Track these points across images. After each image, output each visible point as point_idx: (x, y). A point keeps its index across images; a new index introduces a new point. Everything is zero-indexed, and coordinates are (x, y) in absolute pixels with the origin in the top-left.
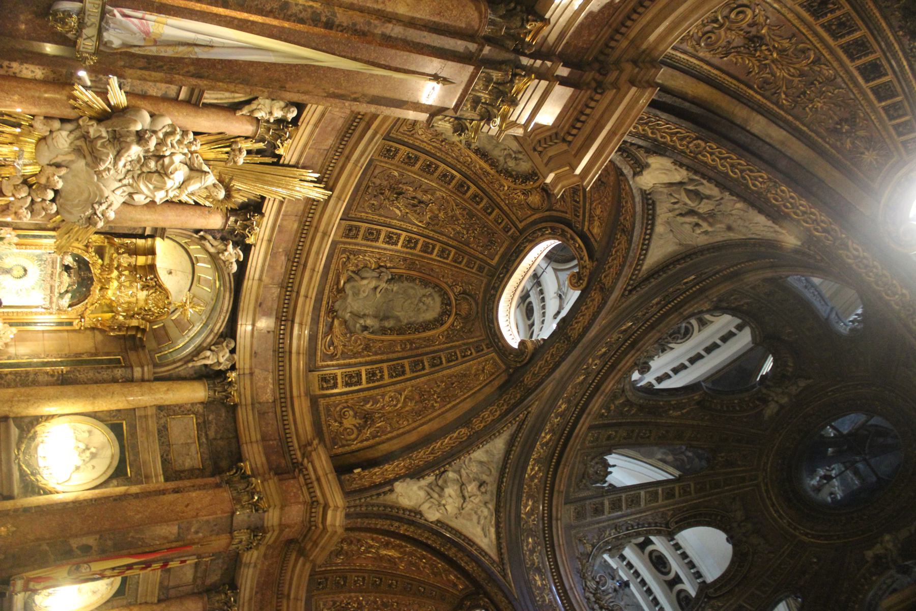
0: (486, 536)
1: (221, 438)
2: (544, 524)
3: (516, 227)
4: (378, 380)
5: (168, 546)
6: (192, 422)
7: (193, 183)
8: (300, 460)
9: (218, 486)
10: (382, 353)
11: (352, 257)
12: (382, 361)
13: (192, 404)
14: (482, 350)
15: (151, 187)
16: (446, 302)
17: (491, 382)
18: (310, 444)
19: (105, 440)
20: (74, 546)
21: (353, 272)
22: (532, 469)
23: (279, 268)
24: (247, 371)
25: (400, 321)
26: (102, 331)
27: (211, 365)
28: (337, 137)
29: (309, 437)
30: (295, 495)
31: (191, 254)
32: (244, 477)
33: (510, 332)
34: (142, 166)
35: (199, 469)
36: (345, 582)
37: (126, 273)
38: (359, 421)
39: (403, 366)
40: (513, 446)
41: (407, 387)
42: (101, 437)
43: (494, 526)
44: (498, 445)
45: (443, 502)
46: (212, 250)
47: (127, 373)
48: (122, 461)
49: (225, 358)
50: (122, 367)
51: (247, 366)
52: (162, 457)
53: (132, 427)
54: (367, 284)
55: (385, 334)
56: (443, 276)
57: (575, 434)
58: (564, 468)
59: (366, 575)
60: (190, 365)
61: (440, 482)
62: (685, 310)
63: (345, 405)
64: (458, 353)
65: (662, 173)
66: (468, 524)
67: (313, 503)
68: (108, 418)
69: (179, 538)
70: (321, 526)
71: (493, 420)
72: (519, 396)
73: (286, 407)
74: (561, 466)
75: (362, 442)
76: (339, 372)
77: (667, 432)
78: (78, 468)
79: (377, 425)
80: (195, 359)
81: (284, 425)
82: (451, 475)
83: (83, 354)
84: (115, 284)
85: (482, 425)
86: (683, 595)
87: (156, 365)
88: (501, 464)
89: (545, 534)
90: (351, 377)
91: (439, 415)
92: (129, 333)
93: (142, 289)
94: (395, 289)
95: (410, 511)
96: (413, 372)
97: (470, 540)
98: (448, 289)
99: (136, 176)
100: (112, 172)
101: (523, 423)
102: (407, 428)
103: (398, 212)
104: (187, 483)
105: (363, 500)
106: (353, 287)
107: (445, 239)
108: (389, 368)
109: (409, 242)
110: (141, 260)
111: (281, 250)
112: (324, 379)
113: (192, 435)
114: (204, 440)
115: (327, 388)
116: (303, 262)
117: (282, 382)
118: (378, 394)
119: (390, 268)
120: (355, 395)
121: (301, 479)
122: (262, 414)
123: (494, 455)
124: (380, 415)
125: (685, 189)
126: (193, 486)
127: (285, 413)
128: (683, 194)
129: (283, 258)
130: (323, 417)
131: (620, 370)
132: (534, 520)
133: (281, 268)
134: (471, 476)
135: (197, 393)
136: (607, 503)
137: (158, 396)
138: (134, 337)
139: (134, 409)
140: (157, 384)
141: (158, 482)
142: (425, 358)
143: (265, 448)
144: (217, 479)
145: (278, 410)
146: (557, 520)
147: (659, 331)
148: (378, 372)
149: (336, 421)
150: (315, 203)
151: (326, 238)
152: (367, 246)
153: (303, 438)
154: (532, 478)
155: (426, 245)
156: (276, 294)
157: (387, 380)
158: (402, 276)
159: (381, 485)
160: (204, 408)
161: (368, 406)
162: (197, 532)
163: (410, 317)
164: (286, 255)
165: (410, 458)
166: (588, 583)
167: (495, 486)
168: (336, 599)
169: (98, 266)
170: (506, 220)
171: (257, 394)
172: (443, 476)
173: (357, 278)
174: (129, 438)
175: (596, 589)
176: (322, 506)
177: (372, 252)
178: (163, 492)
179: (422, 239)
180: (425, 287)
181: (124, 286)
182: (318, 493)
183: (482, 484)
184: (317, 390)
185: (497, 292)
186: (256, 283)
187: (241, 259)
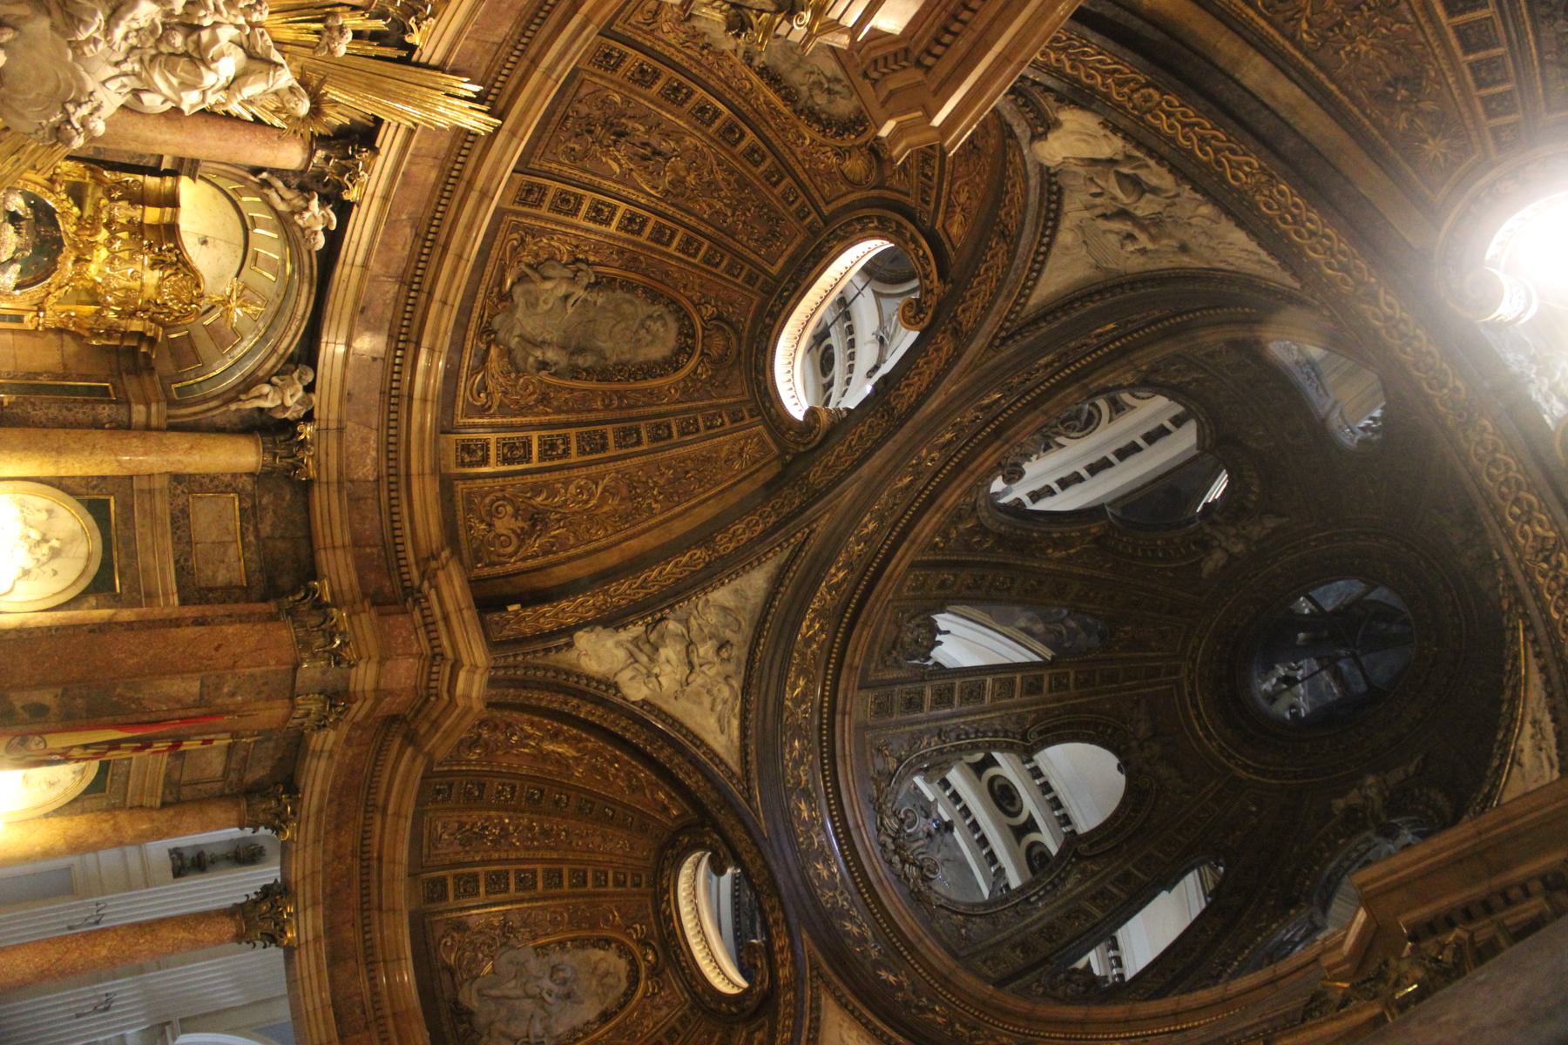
0: (722, 732)
1: (283, 538)
2: (821, 718)
3: (820, 213)
4: (560, 457)
5: (182, 713)
6: (231, 506)
7: (252, 84)
8: (417, 583)
9: (273, 618)
10: (571, 411)
11: (529, 239)
12: (568, 425)
13: (234, 475)
14: (743, 418)
15: (175, 81)
16: (686, 332)
17: (751, 474)
18: (435, 556)
19: (77, 527)
20: (18, 704)
21: (529, 266)
22: (810, 626)
23: (400, 247)
24: (333, 425)
25: (606, 359)
26: (76, 336)
27: (270, 409)
28: (517, 23)
29: (434, 546)
30: (404, 642)
31: (244, 212)
32: (319, 605)
33: (792, 393)
34: (159, 41)
35: (241, 588)
36: (481, 792)
37: (124, 235)
38: (521, 524)
39: (603, 436)
40: (781, 585)
41: (608, 472)
42: (70, 521)
44: (756, 581)
45: (656, 670)
46: (282, 207)
47: (122, 414)
48: (106, 566)
49: (295, 399)
50: (112, 402)
51: (333, 416)
52: (176, 562)
53: (127, 508)
54: (552, 289)
55: (577, 378)
56: (685, 286)
58: (862, 630)
59: (518, 783)
60: (233, 407)
61: (653, 637)
63: (499, 494)
64: (700, 420)
65: (1078, 140)
66: (695, 709)
67: (434, 657)
68: (84, 490)
69: (201, 701)
70: (446, 696)
71: (750, 540)
72: (797, 501)
73: (397, 490)
74: (858, 626)
75: (524, 559)
76: (492, 438)
77: (1040, 583)
78: (26, 573)
79: (553, 533)
80: (243, 397)
81: (393, 521)
82: (672, 626)
83: (40, 374)
84: (103, 253)
85: (732, 546)
86: (1036, 850)
87: (172, 403)
88: (758, 610)
89: (821, 735)
90: (512, 447)
91: (662, 523)
92: (126, 344)
93: (152, 267)
94: (600, 301)
95: (599, 682)
96: (621, 447)
97: (696, 737)
98: (691, 309)
99: (146, 58)
101: (801, 550)
102: (604, 542)
103: (615, 167)
104: (220, 610)
105: (520, 658)
107: (693, 222)
108: (579, 436)
109: (630, 222)
110: (152, 215)
111: (404, 217)
112: (466, 448)
113: (231, 527)
114: (252, 538)
115: (471, 464)
116: (442, 239)
117: (393, 448)
118: (557, 481)
119: (594, 264)
120: (518, 480)
121: (417, 615)
122: (355, 501)
123: (746, 599)
124: (558, 516)
125: (1118, 174)
126: (230, 616)
127: (394, 502)
128: (1113, 179)
129: (408, 230)
130: (460, 514)
131: (972, 473)
132: (805, 712)
133: (403, 249)
134: (706, 631)
135: (243, 456)
136: (928, 693)
137: (174, 457)
138: (134, 350)
139: (131, 477)
140: (173, 437)
141: (169, 604)
142: (642, 424)
143: (356, 558)
144: (272, 606)
145: (384, 495)
146: (844, 714)
147: (1045, 413)
148: (560, 442)
149: (482, 521)
150: (470, 138)
151: (486, 202)
152: (558, 223)
153: (423, 543)
154: (808, 641)
156: (391, 295)
157: (574, 458)
158: (615, 280)
159: (552, 635)
160: (254, 483)
161: (539, 499)
162: (233, 694)
163: (622, 353)
164: (412, 227)
165: (606, 592)
166: (886, 821)
167: (745, 650)
168: (464, 819)
169: (73, 219)
170: (802, 198)
171: (348, 466)
173: (535, 276)
174: (121, 527)
175: (898, 832)
176: (450, 663)
177: (566, 234)
178: (177, 623)
179: (654, 218)
180: (653, 303)
181: (120, 258)
182: (445, 642)
183: (723, 645)
184: (453, 465)
185: (775, 321)
186: (356, 272)
187: (333, 227)
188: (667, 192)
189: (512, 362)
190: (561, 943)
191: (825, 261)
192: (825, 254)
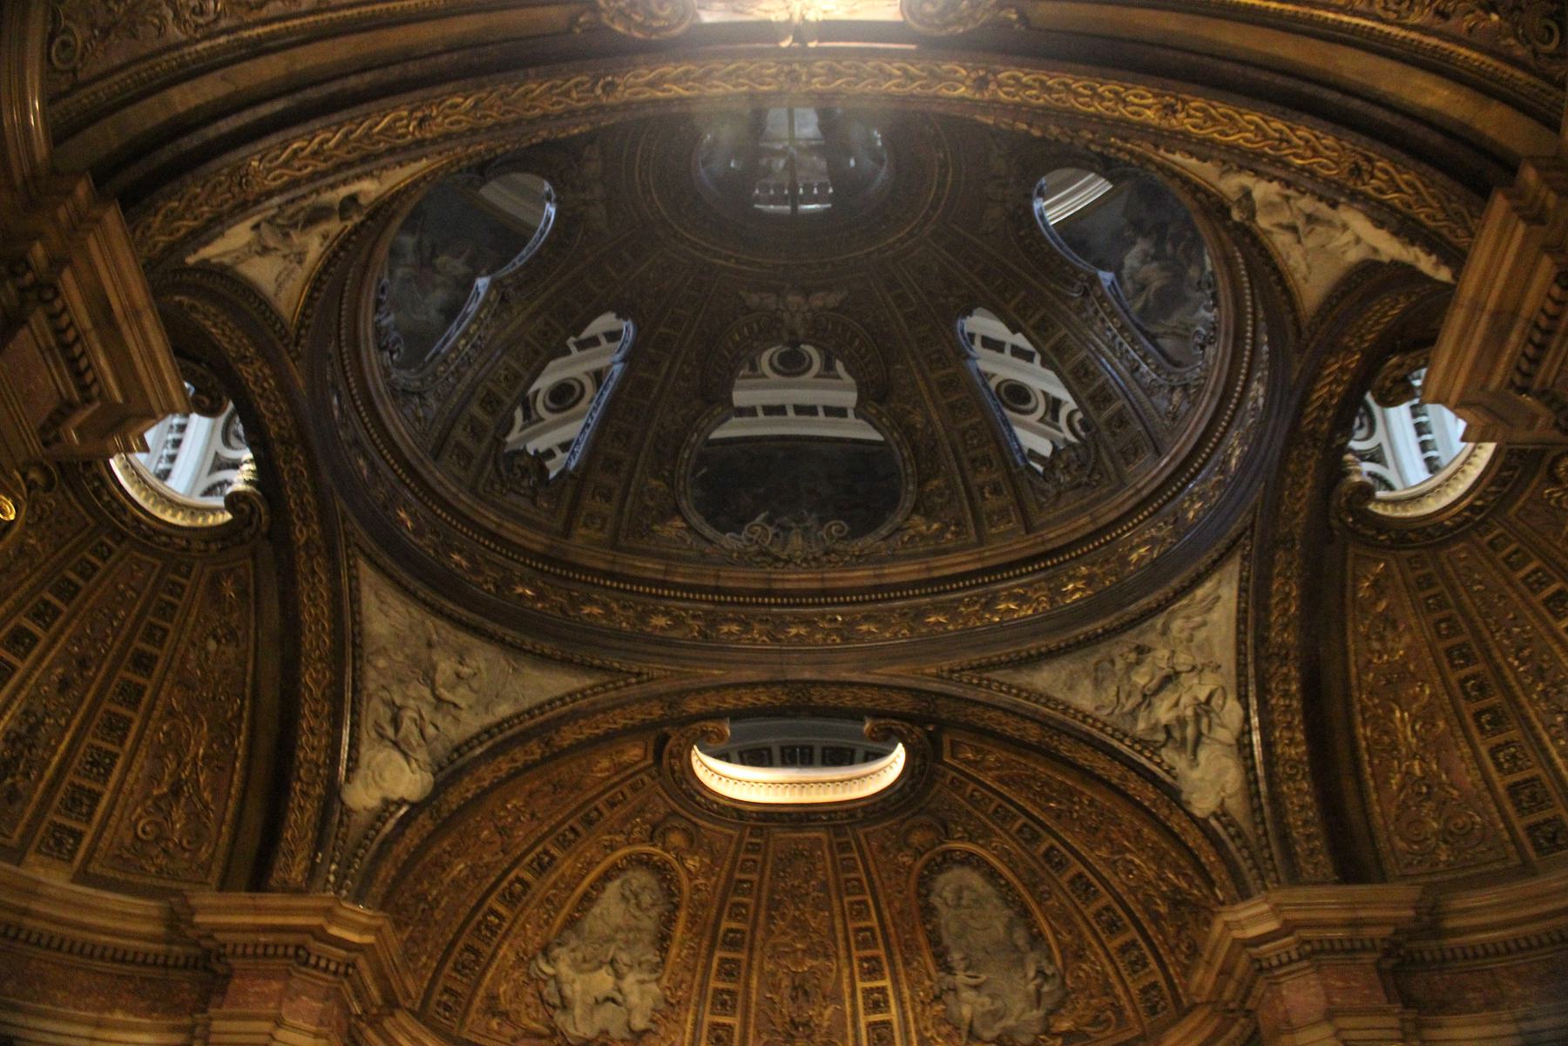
0: (1218, 598)
2: (1161, 506)
3: (741, 838)
4: (1114, 912)
25: (1011, 920)
57: (979, 566)
58: (1050, 540)
62: (656, 571)
66: (1216, 641)
74: (1049, 546)
88: (1079, 653)
106: (984, 1026)
109: (873, 972)
123: (1071, 674)
147: (718, 577)
152: (907, 1032)
155: (864, 944)
163: (996, 907)
170: (742, 856)
172: (1148, 738)
176: (1253, 951)
177: (916, 1021)
179: (855, 954)
180: (935, 908)
188: (827, 957)
189: (1061, 1004)
191: (768, 809)
192: (766, 813)
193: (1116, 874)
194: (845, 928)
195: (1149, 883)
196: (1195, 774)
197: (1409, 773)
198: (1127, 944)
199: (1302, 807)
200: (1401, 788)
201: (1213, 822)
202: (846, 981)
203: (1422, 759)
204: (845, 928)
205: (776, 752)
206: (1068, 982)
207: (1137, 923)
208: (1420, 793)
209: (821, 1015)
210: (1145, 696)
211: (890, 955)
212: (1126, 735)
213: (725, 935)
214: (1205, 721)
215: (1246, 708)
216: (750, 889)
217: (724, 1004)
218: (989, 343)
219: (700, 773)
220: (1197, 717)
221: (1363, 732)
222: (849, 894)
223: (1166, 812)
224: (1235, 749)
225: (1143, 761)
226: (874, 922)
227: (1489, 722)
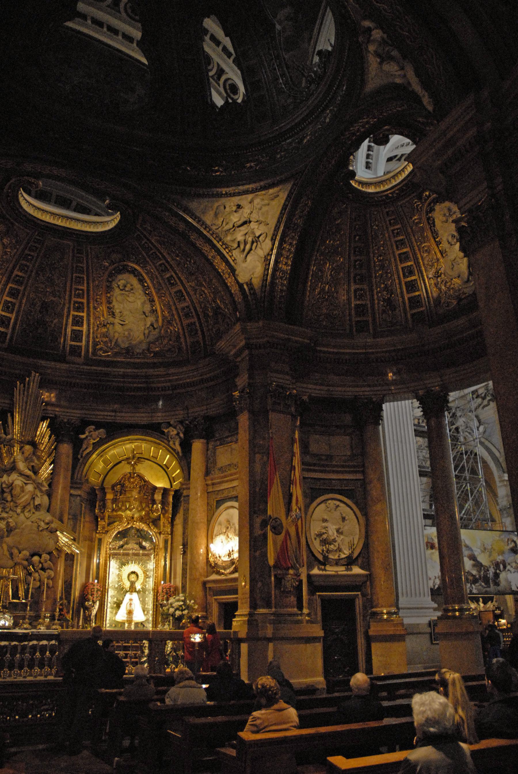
0: (278, 196)
20: (260, 532)
39: (176, 292)
43: (267, 191)
46: (90, 449)
100: (10, 520)
155: (78, 296)
158: (108, 307)
163: (140, 294)
177: (93, 333)
180: (113, 288)
187: (93, 427)
188: (60, 297)
189: (157, 339)
190: (438, 244)
193: (195, 294)
194: (71, 286)
195: (208, 302)
196: (244, 265)
197: (323, 289)
198: (191, 323)
199: (282, 291)
200: (319, 293)
201: (245, 286)
202: (66, 310)
203: (330, 285)
204: (71, 286)
205: (54, 198)
206: (162, 331)
207: (198, 315)
208: (324, 298)
209: (52, 322)
210: (234, 226)
211: (88, 303)
212: (220, 240)
213: (15, 278)
214: (255, 244)
215: (273, 245)
216: (31, 260)
217: (8, 308)
218: (213, 38)
219: (21, 199)
220: (253, 242)
221: (313, 268)
222: (76, 272)
223: (227, 276)
224: (263, 259)
225: (225, 253)
226: (85, 288)
227: (358, 279)
